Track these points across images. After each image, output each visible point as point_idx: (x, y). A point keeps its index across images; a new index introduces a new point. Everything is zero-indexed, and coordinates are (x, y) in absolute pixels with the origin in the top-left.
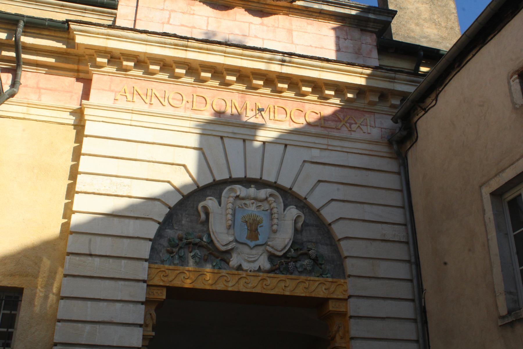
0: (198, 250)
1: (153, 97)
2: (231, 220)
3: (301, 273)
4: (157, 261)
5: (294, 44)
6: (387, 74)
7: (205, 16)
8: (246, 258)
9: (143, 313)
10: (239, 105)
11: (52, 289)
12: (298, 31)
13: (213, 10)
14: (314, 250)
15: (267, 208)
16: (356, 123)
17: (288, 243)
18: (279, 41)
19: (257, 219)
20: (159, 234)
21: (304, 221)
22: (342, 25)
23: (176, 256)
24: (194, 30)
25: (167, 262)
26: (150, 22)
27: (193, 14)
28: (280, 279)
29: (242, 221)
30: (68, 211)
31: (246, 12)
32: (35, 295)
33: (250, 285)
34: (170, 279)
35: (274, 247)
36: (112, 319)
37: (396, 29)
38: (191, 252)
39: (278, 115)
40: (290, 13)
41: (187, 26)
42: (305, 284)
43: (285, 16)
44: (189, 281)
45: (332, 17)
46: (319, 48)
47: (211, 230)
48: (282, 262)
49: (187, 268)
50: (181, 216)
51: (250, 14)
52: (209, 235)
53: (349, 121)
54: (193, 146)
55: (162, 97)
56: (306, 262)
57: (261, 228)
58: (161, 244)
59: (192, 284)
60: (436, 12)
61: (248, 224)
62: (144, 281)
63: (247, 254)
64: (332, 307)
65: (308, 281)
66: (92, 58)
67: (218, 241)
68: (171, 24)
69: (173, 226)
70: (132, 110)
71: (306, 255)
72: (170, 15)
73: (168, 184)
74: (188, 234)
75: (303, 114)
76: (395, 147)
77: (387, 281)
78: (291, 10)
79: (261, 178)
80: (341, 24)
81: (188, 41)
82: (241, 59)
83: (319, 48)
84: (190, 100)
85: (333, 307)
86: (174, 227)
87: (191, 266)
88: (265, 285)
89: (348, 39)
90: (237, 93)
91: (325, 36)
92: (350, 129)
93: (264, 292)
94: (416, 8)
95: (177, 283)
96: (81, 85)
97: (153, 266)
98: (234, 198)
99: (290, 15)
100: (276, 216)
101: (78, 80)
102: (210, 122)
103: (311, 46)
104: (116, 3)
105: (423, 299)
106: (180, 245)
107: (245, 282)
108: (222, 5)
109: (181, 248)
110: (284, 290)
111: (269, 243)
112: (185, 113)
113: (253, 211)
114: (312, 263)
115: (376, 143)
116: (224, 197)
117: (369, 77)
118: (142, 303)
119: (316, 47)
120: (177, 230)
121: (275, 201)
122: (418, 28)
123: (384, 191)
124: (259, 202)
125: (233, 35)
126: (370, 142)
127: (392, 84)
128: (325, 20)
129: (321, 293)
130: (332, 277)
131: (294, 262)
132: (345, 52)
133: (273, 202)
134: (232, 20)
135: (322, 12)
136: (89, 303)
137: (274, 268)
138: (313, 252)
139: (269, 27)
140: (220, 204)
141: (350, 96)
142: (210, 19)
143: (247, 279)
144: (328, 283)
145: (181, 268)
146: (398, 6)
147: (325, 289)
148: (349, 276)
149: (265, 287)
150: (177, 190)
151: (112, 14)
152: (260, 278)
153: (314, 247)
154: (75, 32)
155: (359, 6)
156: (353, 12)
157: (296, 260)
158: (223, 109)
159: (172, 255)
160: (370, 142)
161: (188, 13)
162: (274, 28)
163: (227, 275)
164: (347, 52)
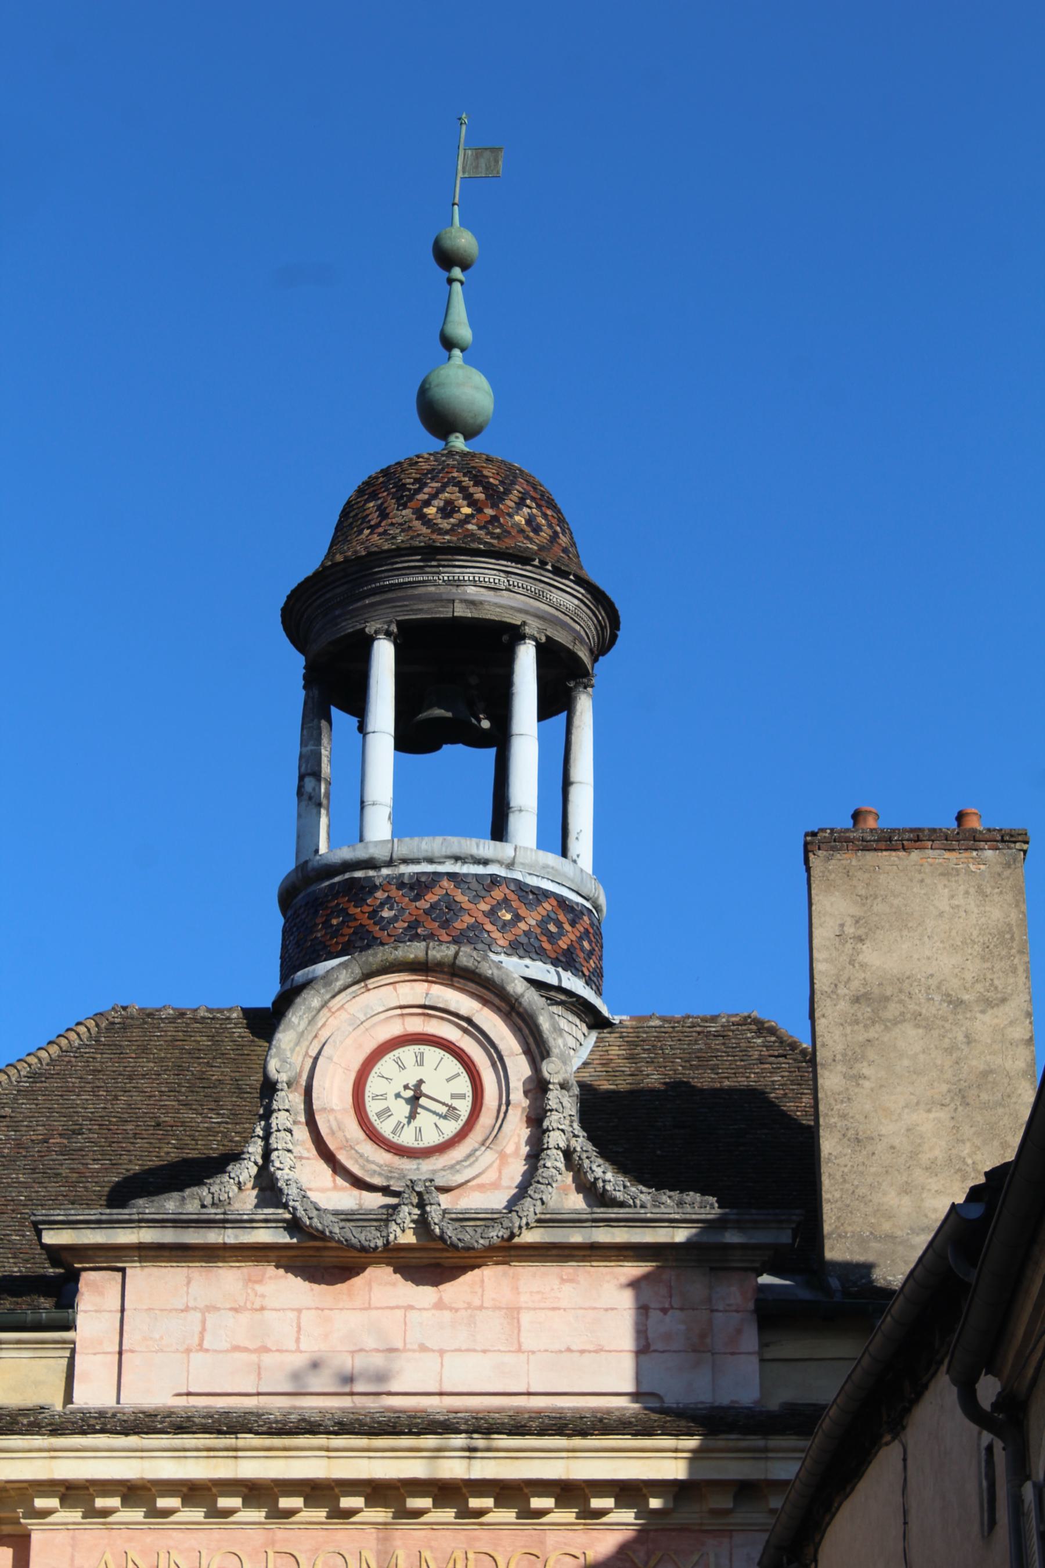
5: (523, 1352)
7: (293, 1310)
12: (535, 1309)
13: (312, 1284)
18: (484, 1351)
24: (267, 1359)
26: (156, 1352)
27: (262, 1309)
31: (398, 1276)
37: (839, 1218)
40: (512, 1258)
41: (246, 1350)
43: (500, 1268)
45: (626, 1253)
46: (590, 1352)
51: (406, 1280)
60: (967, 1131)
66: (25, 1494)
68: (207, 1350)
72: (204, 1322)
78: (513, 1253)
80: (654, 1264)
81: (237, 1438)
82: (370, 1458)
83: (590, 1352)
89: (672, 1308)
90: (373, 1530)
91: (610, 1311)
94: (908, 1130)
103: (569, 1350)
104: (71, 1317)
117: (696, 1457)
119: (582, 1352)
122: (906, 1200)
125: (363, 1354)
128: (610, 1261)
134: (361, 1309)
139: (457, 1310)
141: (655, 1503)
146: (851, 1133)
151: (64, 1342)
155: (694, 1217)
156: (681, 1235)
161: (249, 1306)
162: (469, 1311)
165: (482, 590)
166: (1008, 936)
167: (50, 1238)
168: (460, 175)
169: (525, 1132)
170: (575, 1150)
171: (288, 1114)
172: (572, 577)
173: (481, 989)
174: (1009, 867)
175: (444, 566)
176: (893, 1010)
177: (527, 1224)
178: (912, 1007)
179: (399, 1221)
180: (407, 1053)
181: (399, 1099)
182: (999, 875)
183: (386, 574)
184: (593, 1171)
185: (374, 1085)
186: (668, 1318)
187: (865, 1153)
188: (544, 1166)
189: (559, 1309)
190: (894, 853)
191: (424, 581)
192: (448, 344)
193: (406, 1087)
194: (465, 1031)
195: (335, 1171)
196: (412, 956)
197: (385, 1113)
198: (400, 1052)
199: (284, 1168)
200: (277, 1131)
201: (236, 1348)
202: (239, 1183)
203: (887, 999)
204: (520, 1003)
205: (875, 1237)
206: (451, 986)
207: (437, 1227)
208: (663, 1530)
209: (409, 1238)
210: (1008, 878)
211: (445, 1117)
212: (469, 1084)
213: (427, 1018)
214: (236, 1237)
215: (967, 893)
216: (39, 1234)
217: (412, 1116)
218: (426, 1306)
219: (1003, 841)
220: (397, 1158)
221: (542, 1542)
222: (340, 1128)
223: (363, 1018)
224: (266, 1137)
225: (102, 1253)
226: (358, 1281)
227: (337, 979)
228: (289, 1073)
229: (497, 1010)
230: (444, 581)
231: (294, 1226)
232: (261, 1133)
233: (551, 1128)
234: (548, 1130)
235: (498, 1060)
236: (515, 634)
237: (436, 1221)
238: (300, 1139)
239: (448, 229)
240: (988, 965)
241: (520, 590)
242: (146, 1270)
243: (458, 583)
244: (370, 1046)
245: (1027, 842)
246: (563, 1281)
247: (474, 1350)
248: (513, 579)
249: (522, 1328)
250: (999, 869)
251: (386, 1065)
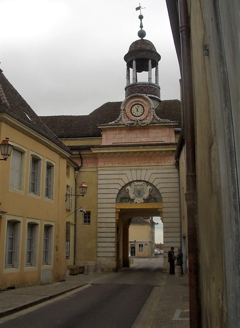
20: (117, 196)
56: (152, 200)
74: (124, 196)
95: (122, 208)
129: (156, 207)
140: (131, 187)
157: (150, 199)
186: (165, 133)
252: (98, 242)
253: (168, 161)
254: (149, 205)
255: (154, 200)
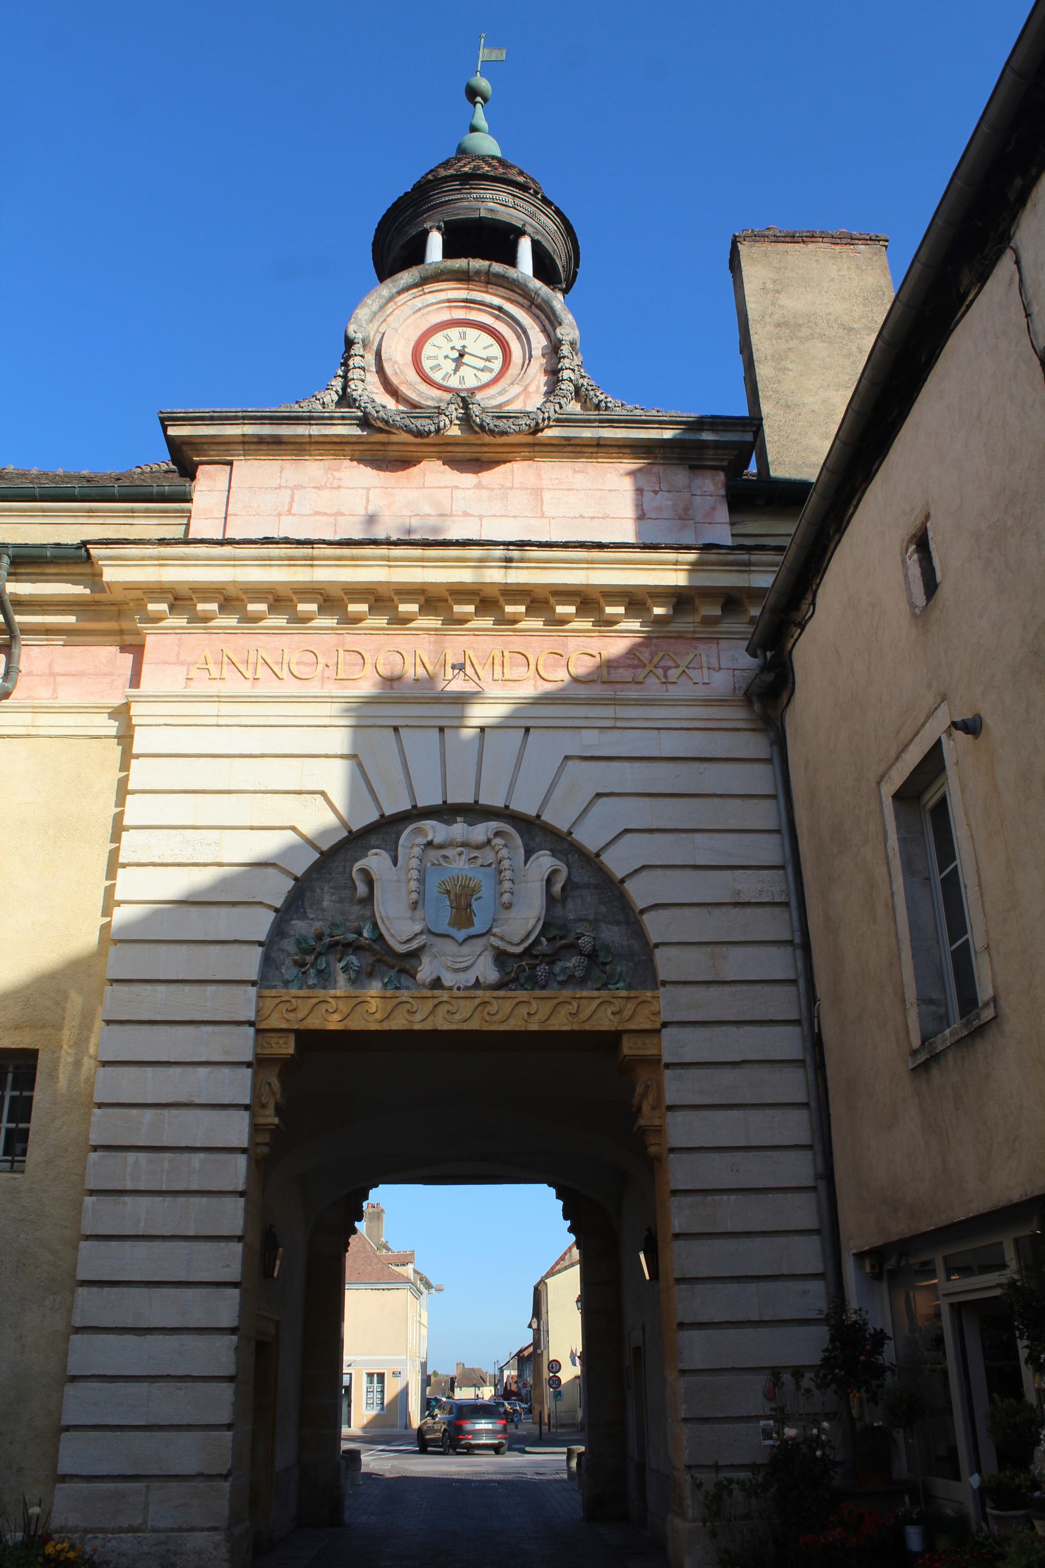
0: (355, 955)
1: (259, 666)
2: (415, 891)
3: (563, 984)
4: (277, 983)
6: (731, 558)
7: (363, 488)
8: (449, 964)
9: (249, 1083)
10: (429, 658)
11: (87, 1048)
12: (554, 489)
13: (379, 472)
14: (588, 936)
15: (491, 861)
16: (678, 666)
17: (534, 928)
18: (515, 517)
19: (469, 884)
20: (278, 931)
21: (569, 879)
22: (649, 463)
23: (312, 971)
25: (295, 983)
27: (339, 487)
28: (518, 1000)
29: (438, 892)
30: (109, 903)
31: (447, 467)
32: (57, 1060)
33: (457, 1017)
34: (300, 1016)
35: (506, 938)
36: (192, 1099)
38: (340, 961)
39: (511, 669)
40: (536, 454)
41: (325, 514)
42: (571, 1007)
44: (336, 1017)
46: (598, 518)
47: (377, 915)
48: (522, 965)
49: (332, 992)
50: (320, 891)
52: (375, 925)
53: (661, 664)
54: (339, 753)
55: (277, 663)
56: (573, 961)
57: (479, 901)
58: (283, 950)
59: (342, 1022)
61: (453, 897)
62: (251, 1024)
63: (452, 956)
64: (628, 1047)
65: (577, 1000)
66: (142, 605)
67: (392, 935)
68: (294, 515)
69: (305, 912)
70: (218, 696)
71: (573, 947)
73: (290, 833)
74: (334, 925)
75: (564, 662)
76: (757, 706)
77: (744, 988)
78: (536, 449)
79: (476, 802)
81: (313, 548)
82: (423, 567)
83: (598, 518)
84: (331, 662)
85: (630, 1048)
86: (308, 915)
87: (342, 986)
88: (488, 1013)
89: (661, 490)
90: (426, 636)
91: (613, 492)
92: (664, 680)
93: (486, 1027)
95: (314, 1023)
96: (129, 658)
97: (266, 993)
98: (422, 847)
99: (536, 459)
100: (507, 874)
101: (124, 648)
102: (371, 701)
103: (581, 516)
104: (187, 490)
105: (816, 1019)
106: (318, 949)
107: (448, 1011)
108: (397, 461)
109: (320, 954)
110: (526, 1021)
111: (494, 930)
112: (322, 688)
113: (461, 869)
114: (586, 962)
115: (721, 702)
116: (403, 846)
117: (695, 567)
118: (249, 1065)
119: (592, 518)
120: (312, 919)
121: (505, 846)
123: (738, 801)
124: (474, 851)
126: (707, 702)
127: (745, 576)
128: (612, 458)
129: (605, 1021)
130: (629, 987)
131: (548, 964)
132: (657, 519)
133: (501, 847)
134: (417, 488)
135: (602, 443)
136: (149, 1070)
137: (507, 978)
138: (586, 940)
139: (492, 490)
140: (395, 862)
141: (658, 611)
142: (371, 492)
143: (452, 1005)
144: (619, 1000)
145: (323, 992)
147: (613, 1013)
148: (664, 983)
149: (487, 1018)
150: (310, 842)
151: (182, 511)
152: (477, 1001)
153: (591, 929)
154: (100, 563)
155: (678, 419)
156: (668, 434)
157: (551, 959)
158: (397, 672)
159: (303, 970)
160: (707, 702)
162: (502, 490)
163: (410, 1000)
164: (661, 519)
165: (498, 205)
166: (880, 293)
167: (172, 431)
168: (481, 59)
169: (544, 379)
170: (583, 385)
171: (361, 358)
172: (553, 208)
173: (508, 292)
174: (877, 255)
175: (474, 189)
176: (805, 332)
177: (549, 418)
178: (818, 330)
179: (447, 413)
180: (454, 332)
181: (447, 359)
182: (870, 259)
183: (438, 196)
184: (597, 397)
185: (428, 350)
187: (793, 413)
188: (560, 389)
189: (573, 490)
190: (796, 245)
191: (462, 199)
192: (474, 129)
193: (453, 348)
194: (497, 318)
195: (397, 401)
196: (457, 266)
197: (437, 367)
198: (448, 331)
199: (356, 389)
200: (353, 368)
201: (317, 513)
202: (324, 403)
203: (800, 326)
204: (538, 295)
205: (806, 465)
206: (487, 292)
207: (478, 418)
208: (663, 637)
209: (455, 431)
210: (877, 261)
211: (482, 370)
212: (500, 350)
213: (468, 310)
214: (319, 430)
215: (849, 268)
216: (165, 428)
217: (456, 370)
218: (469, 487)
219: (871, 239)
220: (446, 393)
221: (565, 645)
222: (402, 373)
223: (420, 306)
224: (345, 377)
225: (214, 447)
226: (414, 470)
227: (401, 278)
228: (364, 333)
229: (521, 306)
230: (474, 198)
231: (365, 422)
232: (341, 374)
233: (564, 368)
234: (562, 369)
235: (522, 333)
236: (520, 232)
237: (477, 414)
238: (372, 381)
239: (474, 78)
240: (869, 309)
241: (521, 209)
242: (249, 462)
243: (482, 200)
244: (425, 326)
245: (887, 241)
246: (575, 471)
247: (507, 516)
248: (517, 201)
249: (544, 502)
250: (869, 256)
251: (438, 338)
252: (79, 1330)
253: (694, 674)
254: (546, 1008)
255: (588, 969)
